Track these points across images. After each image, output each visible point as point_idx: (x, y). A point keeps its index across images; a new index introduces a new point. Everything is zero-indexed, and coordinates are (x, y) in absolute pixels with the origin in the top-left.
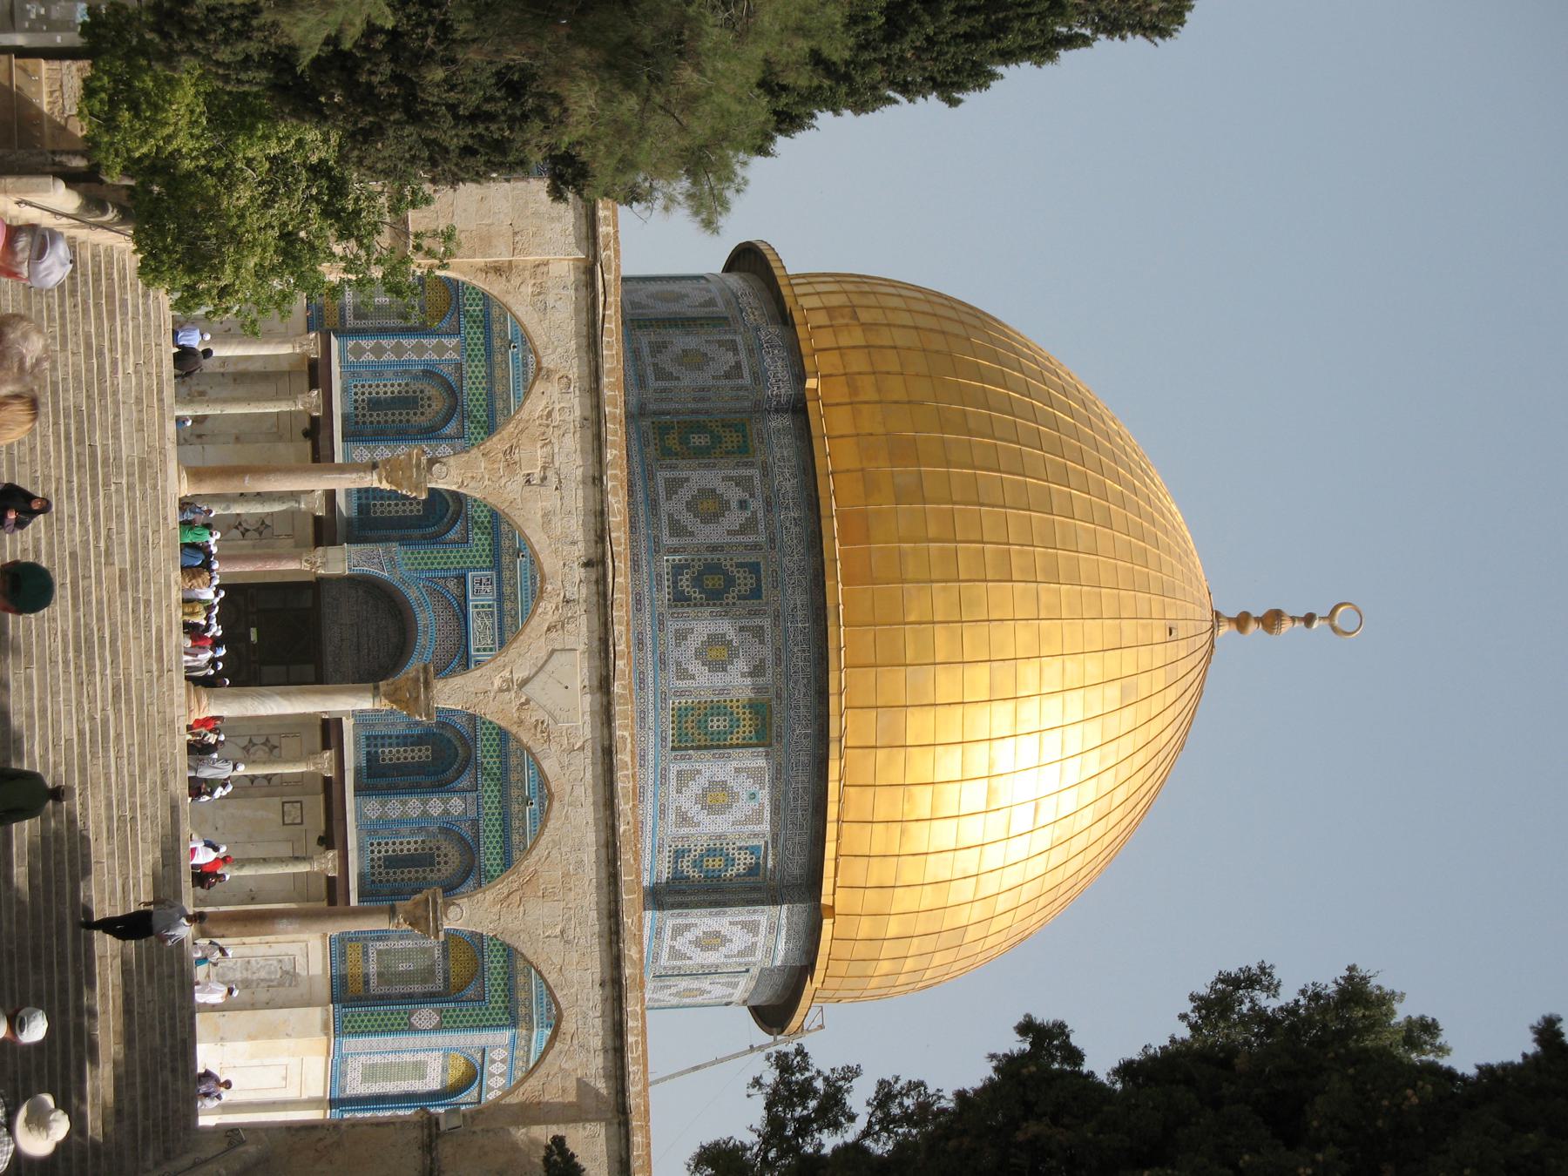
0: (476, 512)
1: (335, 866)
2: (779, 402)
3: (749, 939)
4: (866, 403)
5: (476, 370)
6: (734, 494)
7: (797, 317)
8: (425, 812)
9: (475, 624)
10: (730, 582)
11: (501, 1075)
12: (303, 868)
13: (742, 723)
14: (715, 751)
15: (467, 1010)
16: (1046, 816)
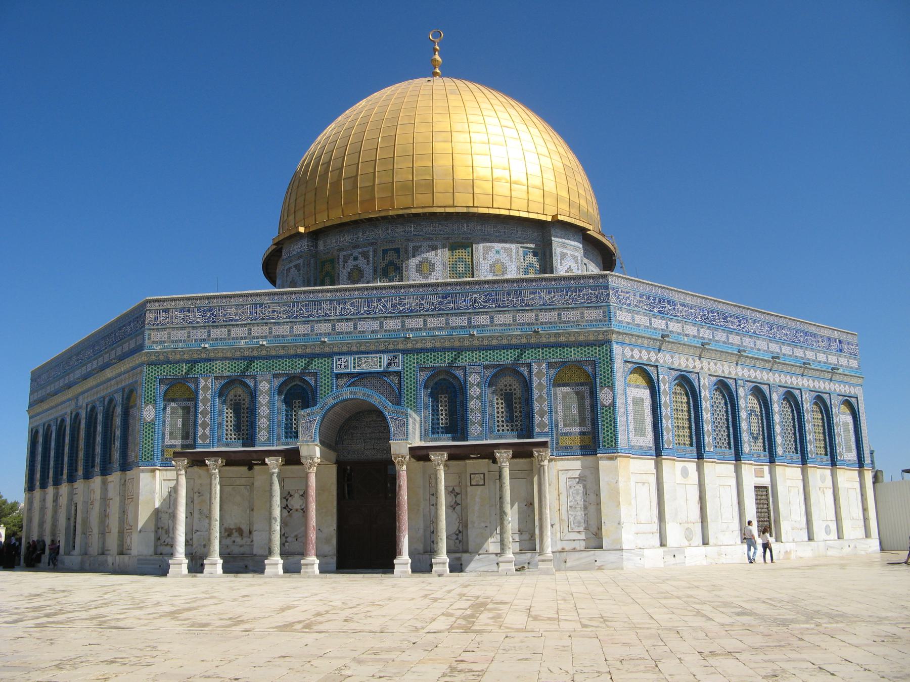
0: (299, 368)
1: (505, 452)
2: (312, 246)
3: (569, 257)
4: (315, 208)
5: (218, 368)
6: (351, 263)
7: (277, 241)
8: (478, 398)
9: (365, 368)
10: (391, 263)
11: (640, 352)
12: (506, 473)
13: (461, 256)
14: (475, 269)
15: (601, 371)
16: (510, 124)
